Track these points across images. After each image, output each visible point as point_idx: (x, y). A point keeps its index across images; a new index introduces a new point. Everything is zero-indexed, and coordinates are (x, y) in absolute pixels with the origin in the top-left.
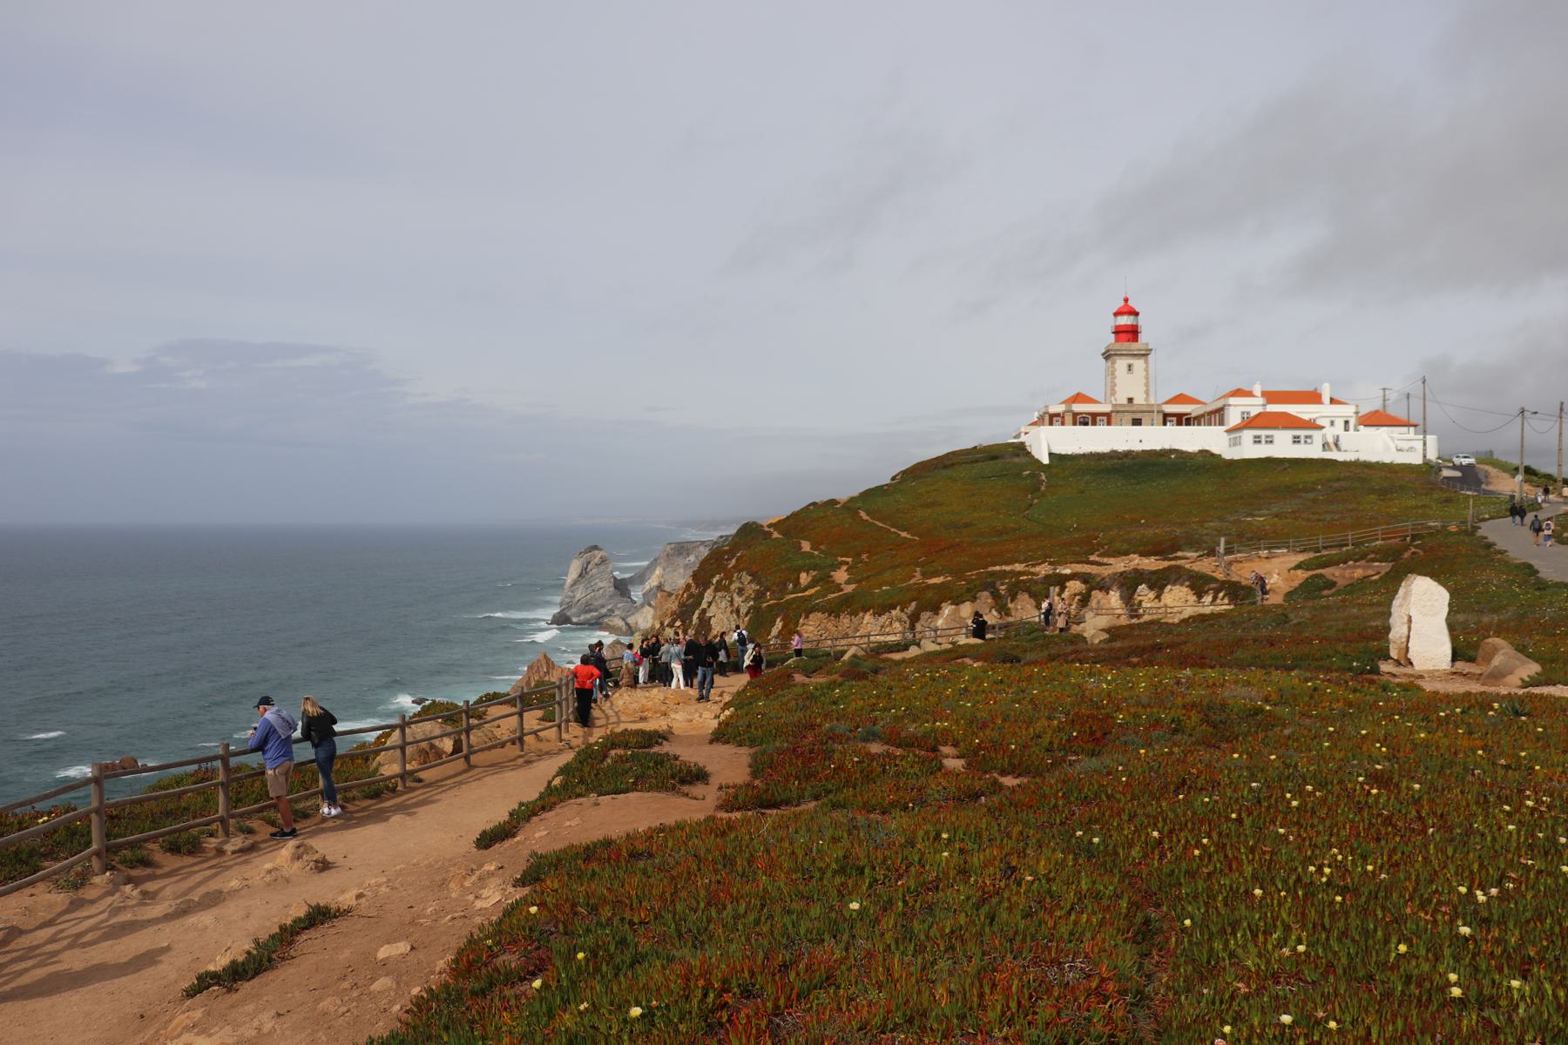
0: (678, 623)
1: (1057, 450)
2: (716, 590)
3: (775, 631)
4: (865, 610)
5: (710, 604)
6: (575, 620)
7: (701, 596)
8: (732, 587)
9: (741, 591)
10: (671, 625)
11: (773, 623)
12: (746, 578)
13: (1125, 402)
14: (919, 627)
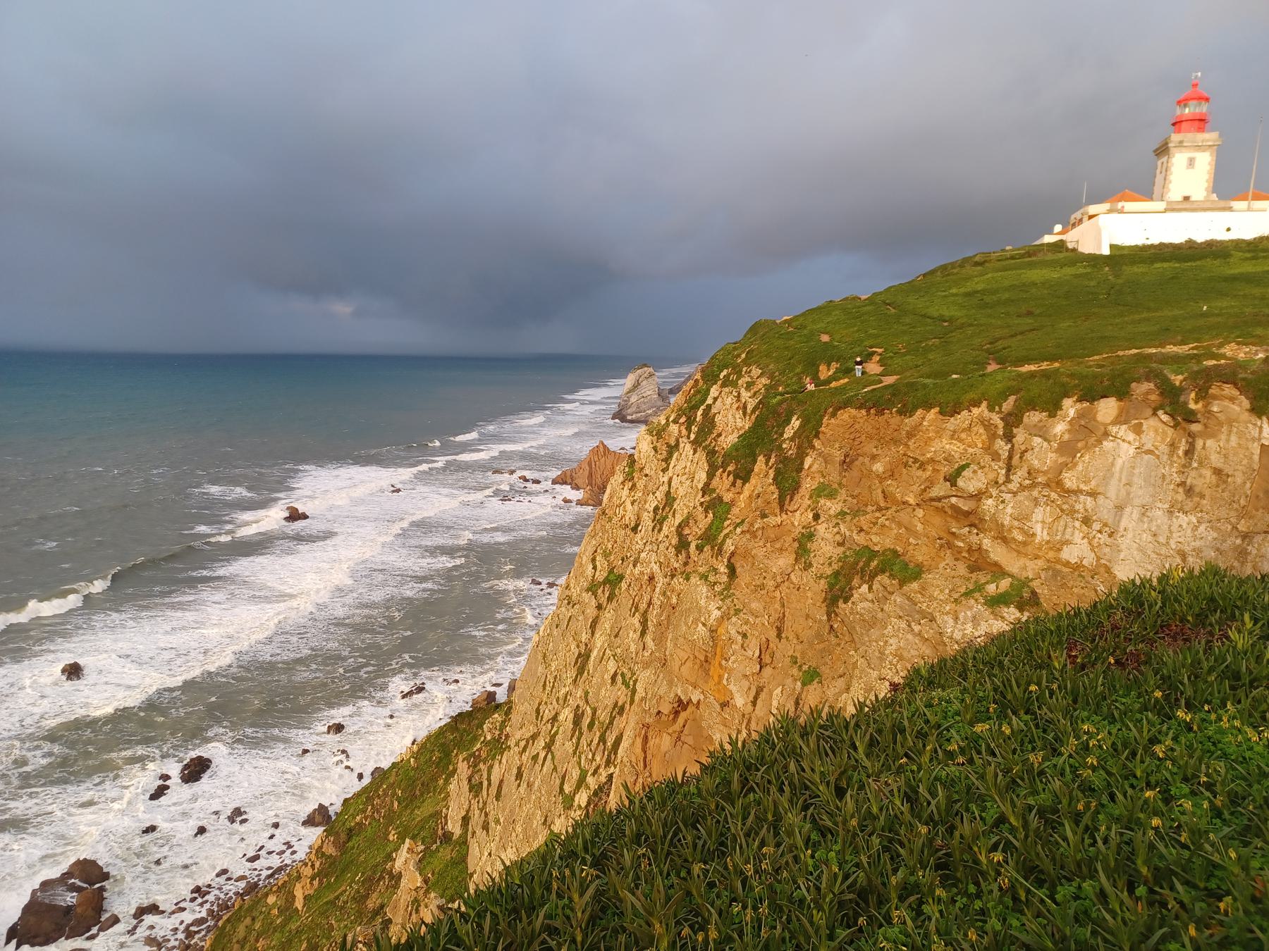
0: (683, 420)
1: (1119, 241)
2: (723, 385)
3: (789, 432)
4: (928, 407)
5: (715, 399)
6: (629, 418)
7: (708, 391)
8: (740, 382)
9: (749, 386)
10: (675, 422)
11: (788, 422)
12: (756, 371)
13: (1180, 199)
14: (1020, 435)
